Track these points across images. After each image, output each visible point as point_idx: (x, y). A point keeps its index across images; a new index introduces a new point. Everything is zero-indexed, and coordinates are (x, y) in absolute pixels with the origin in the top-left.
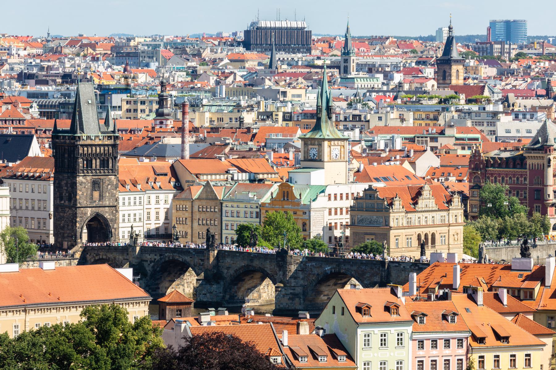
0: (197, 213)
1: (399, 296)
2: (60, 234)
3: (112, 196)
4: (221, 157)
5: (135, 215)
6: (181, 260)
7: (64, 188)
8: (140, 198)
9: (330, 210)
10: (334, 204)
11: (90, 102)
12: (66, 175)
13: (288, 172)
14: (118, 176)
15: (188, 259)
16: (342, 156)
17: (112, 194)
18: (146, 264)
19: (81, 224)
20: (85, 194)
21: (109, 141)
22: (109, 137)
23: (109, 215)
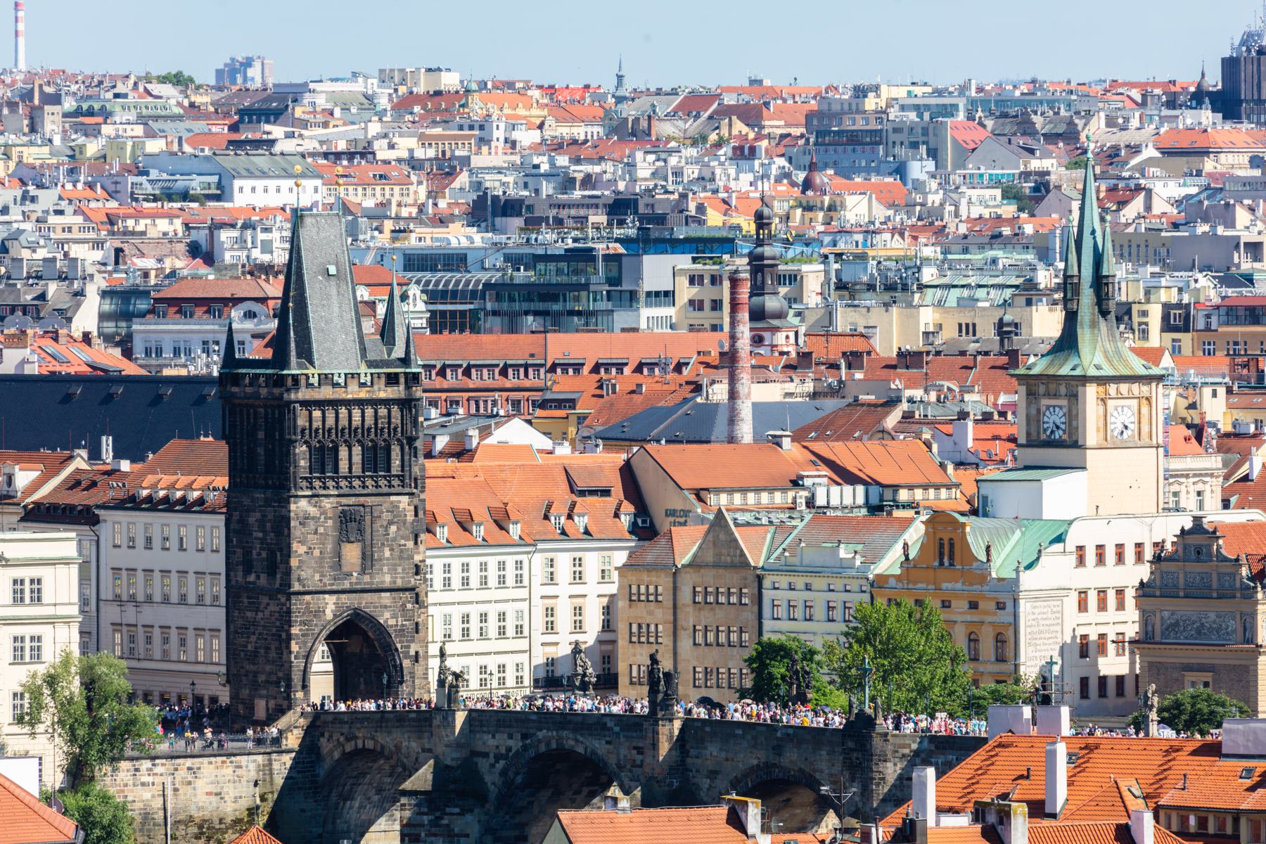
0: (690, 609)
1: (750, 831)
2: (246, 675)
3: (401, 558)
4: (781, 436)
5: (502, 617)
6: (580, 750)
7: (255, 534)
8: (519, 565)
9: (1083, 593)
10: (1093, 577)
11: (333, 270)
12: (259, 495)
13: (977, 481)
14: (422, 496)
15: (599, 746)
16: (1145, 429)
17: (402, 551)
18: (483, 764)
19: (305, 643)
20: (317, 553)
21: (389, 389)
22: (388, 375)
23: (394, 616)
